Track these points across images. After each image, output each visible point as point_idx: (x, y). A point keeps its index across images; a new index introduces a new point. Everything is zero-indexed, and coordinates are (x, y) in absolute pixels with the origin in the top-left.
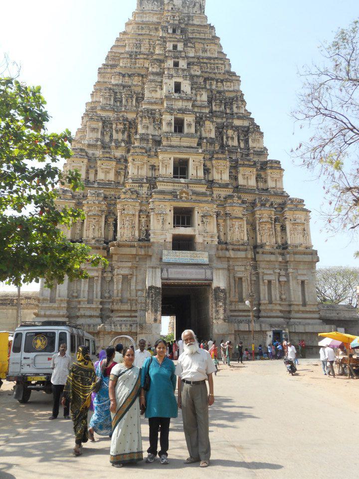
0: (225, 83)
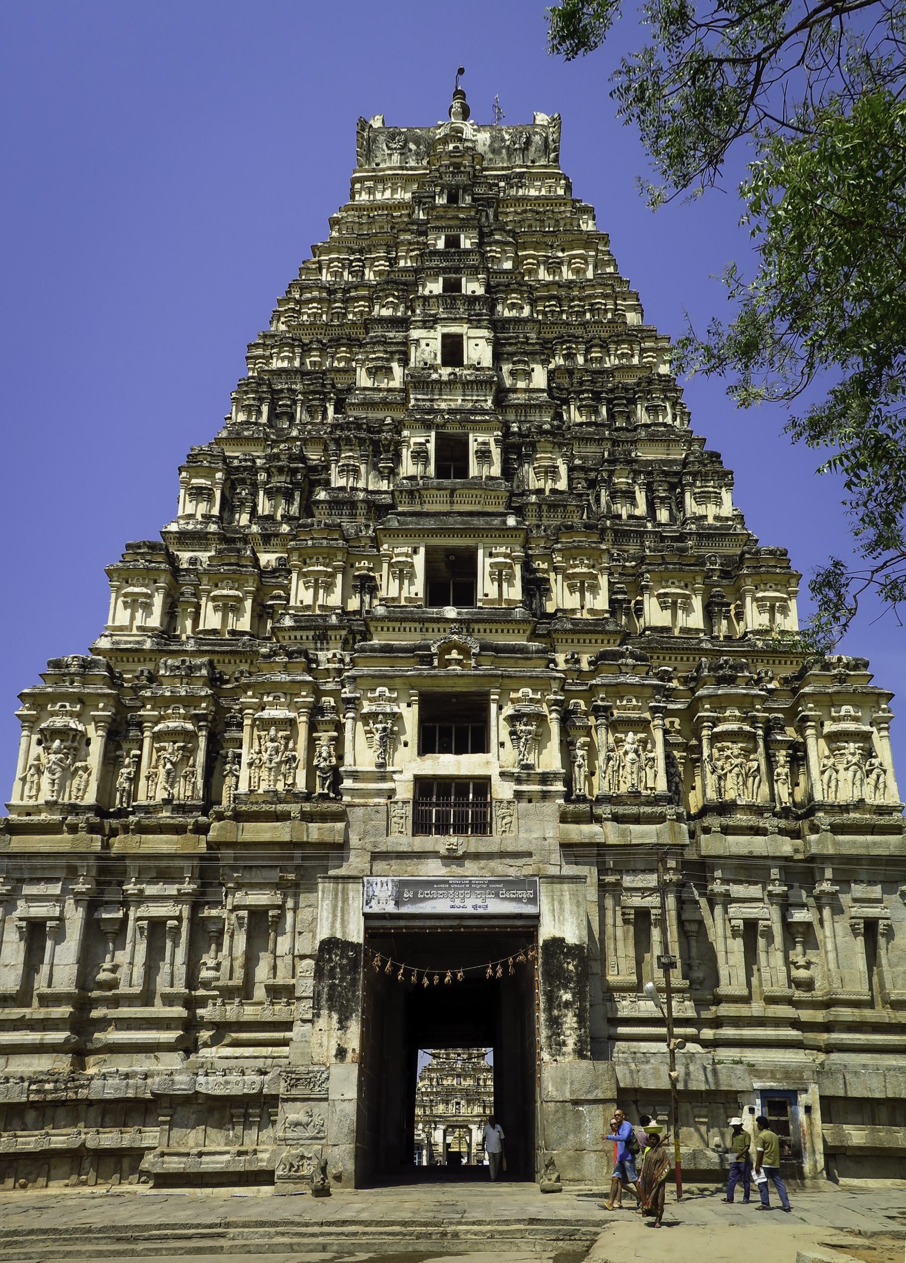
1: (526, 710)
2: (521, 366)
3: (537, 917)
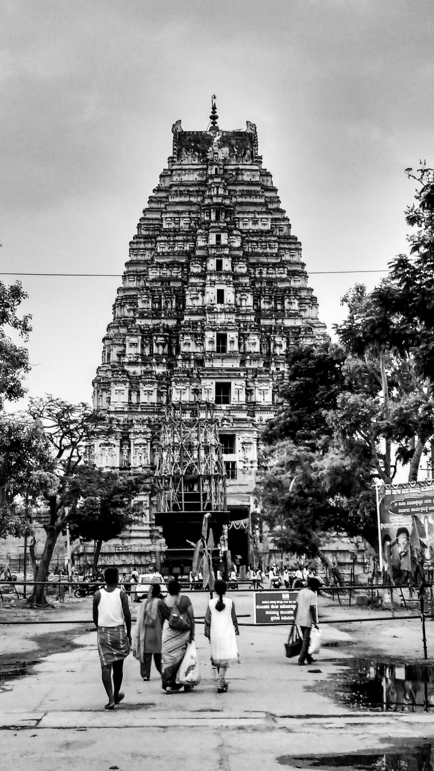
0: (277, 269)
1: (246, 441)
2: (244, 297)
3: (249, 506)
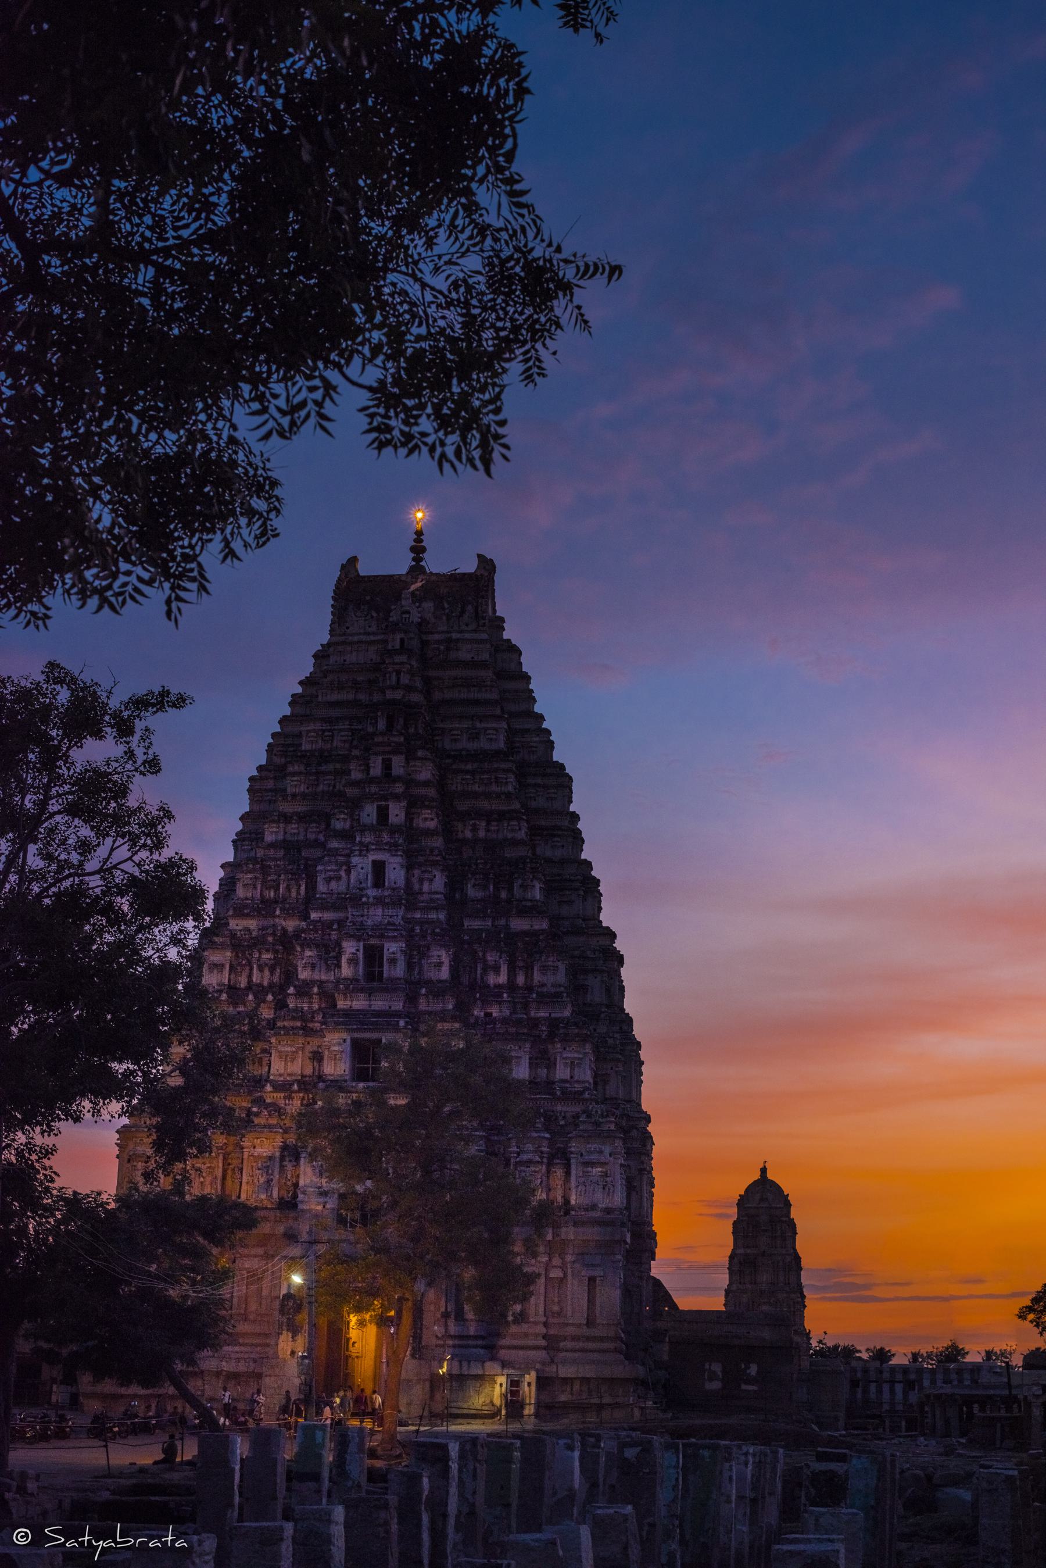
2: (427, 875)
